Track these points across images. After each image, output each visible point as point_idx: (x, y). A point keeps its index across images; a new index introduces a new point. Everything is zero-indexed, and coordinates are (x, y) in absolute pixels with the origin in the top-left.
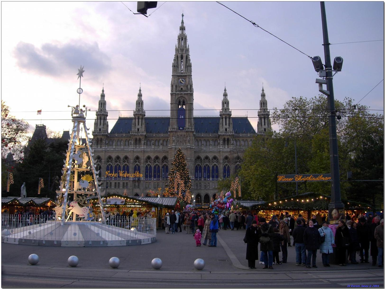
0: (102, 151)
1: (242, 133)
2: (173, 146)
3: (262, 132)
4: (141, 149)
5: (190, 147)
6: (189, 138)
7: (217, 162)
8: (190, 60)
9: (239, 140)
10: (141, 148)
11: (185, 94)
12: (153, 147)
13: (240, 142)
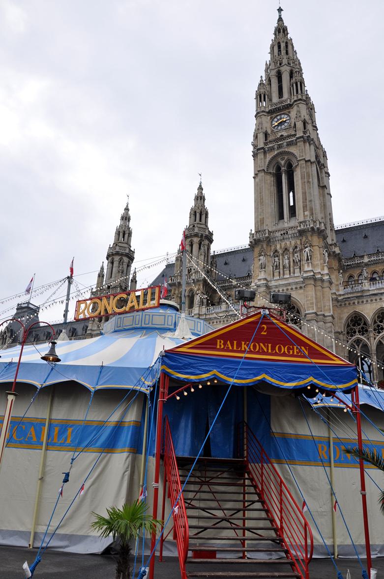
2: (260, 280)
6: (307, 250)
10: (193, 315)
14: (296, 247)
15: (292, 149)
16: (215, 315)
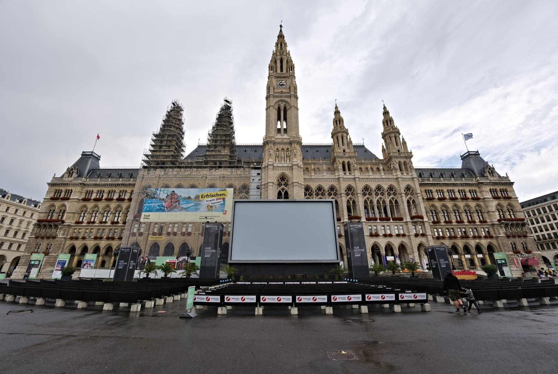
6: (295, 151)
14: (288, 149)
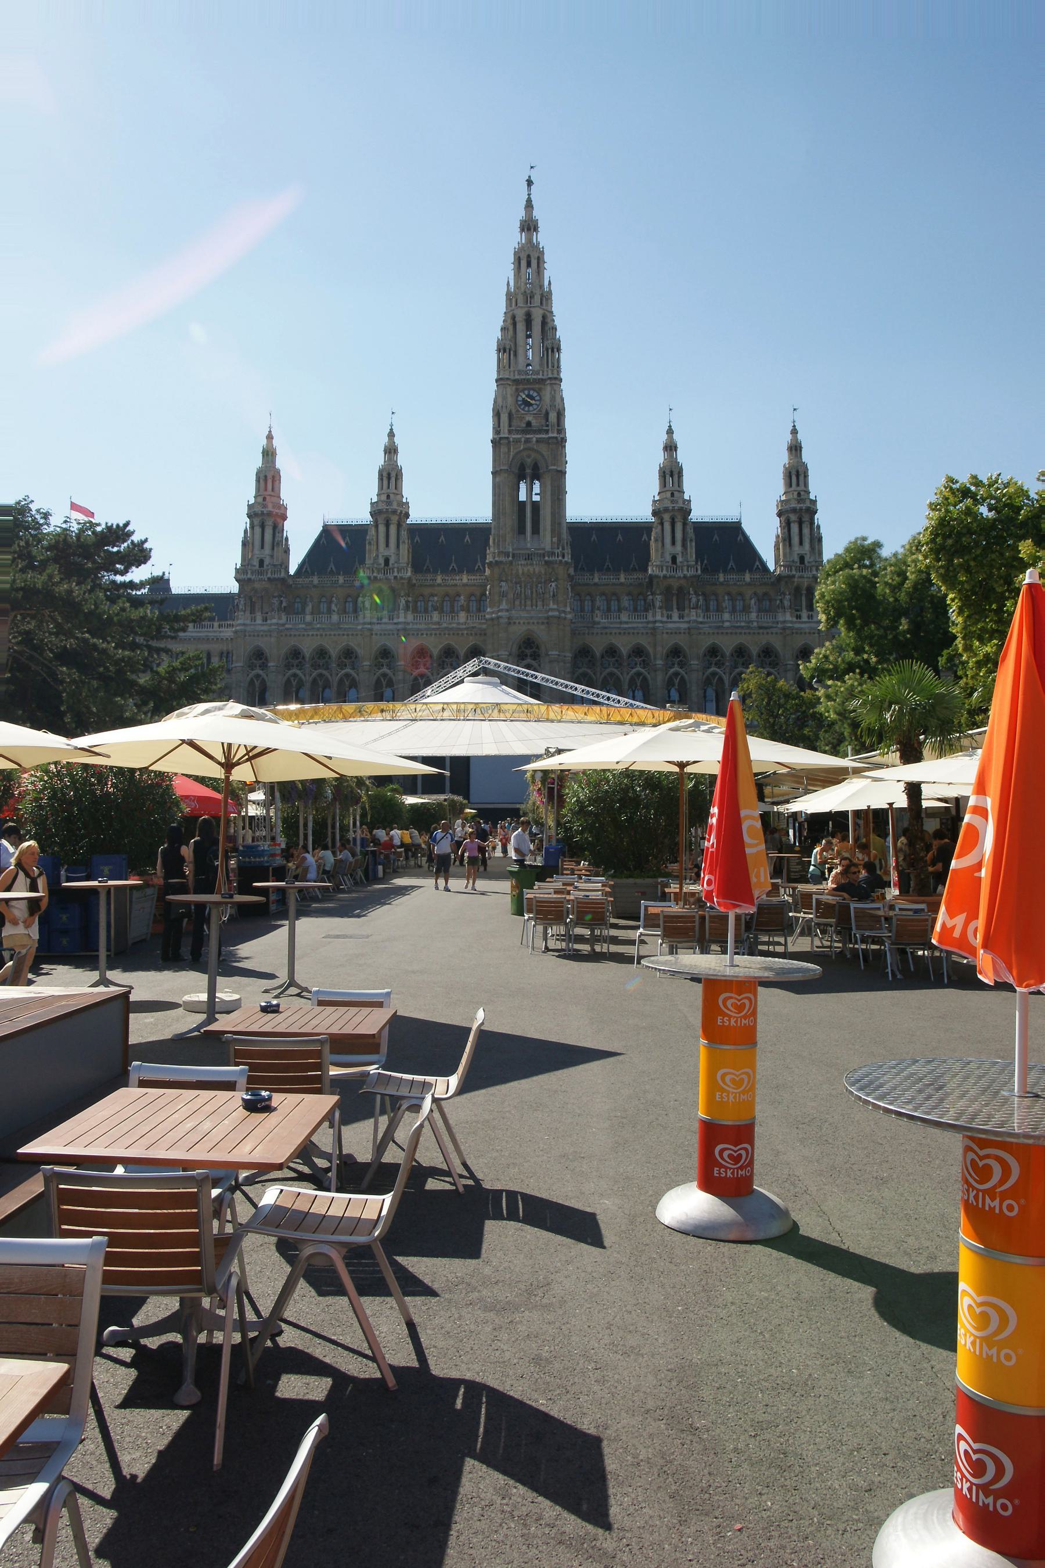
0: (269, 631)
1: (725, 572)
2: (501, 610)
3: (793, 568)
4: (395, 624)
5: (556, 613)
6: (553, 584)
7: (645, 664)
8: (556, 329)
9: (716, 594)
10: (395, 621)
11: (538, 441)
12: (436, 617)
13: (717, 600)
15: (543, 449)
16: (423, 626)
